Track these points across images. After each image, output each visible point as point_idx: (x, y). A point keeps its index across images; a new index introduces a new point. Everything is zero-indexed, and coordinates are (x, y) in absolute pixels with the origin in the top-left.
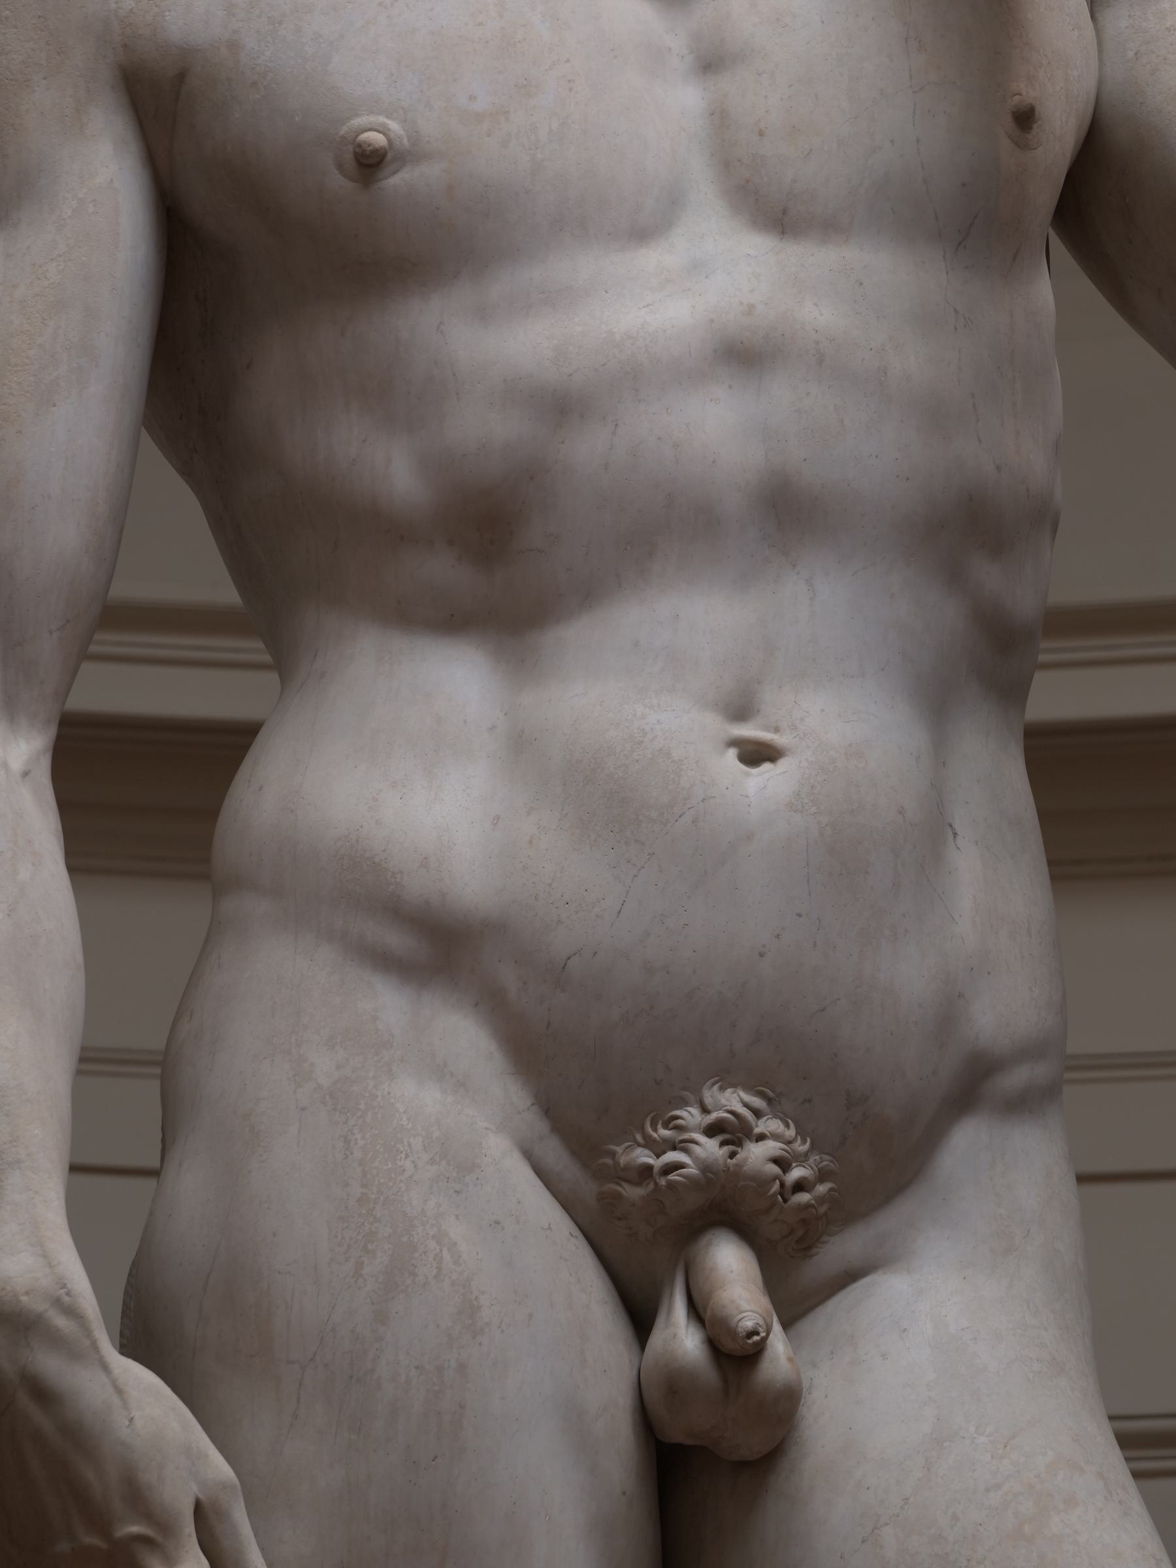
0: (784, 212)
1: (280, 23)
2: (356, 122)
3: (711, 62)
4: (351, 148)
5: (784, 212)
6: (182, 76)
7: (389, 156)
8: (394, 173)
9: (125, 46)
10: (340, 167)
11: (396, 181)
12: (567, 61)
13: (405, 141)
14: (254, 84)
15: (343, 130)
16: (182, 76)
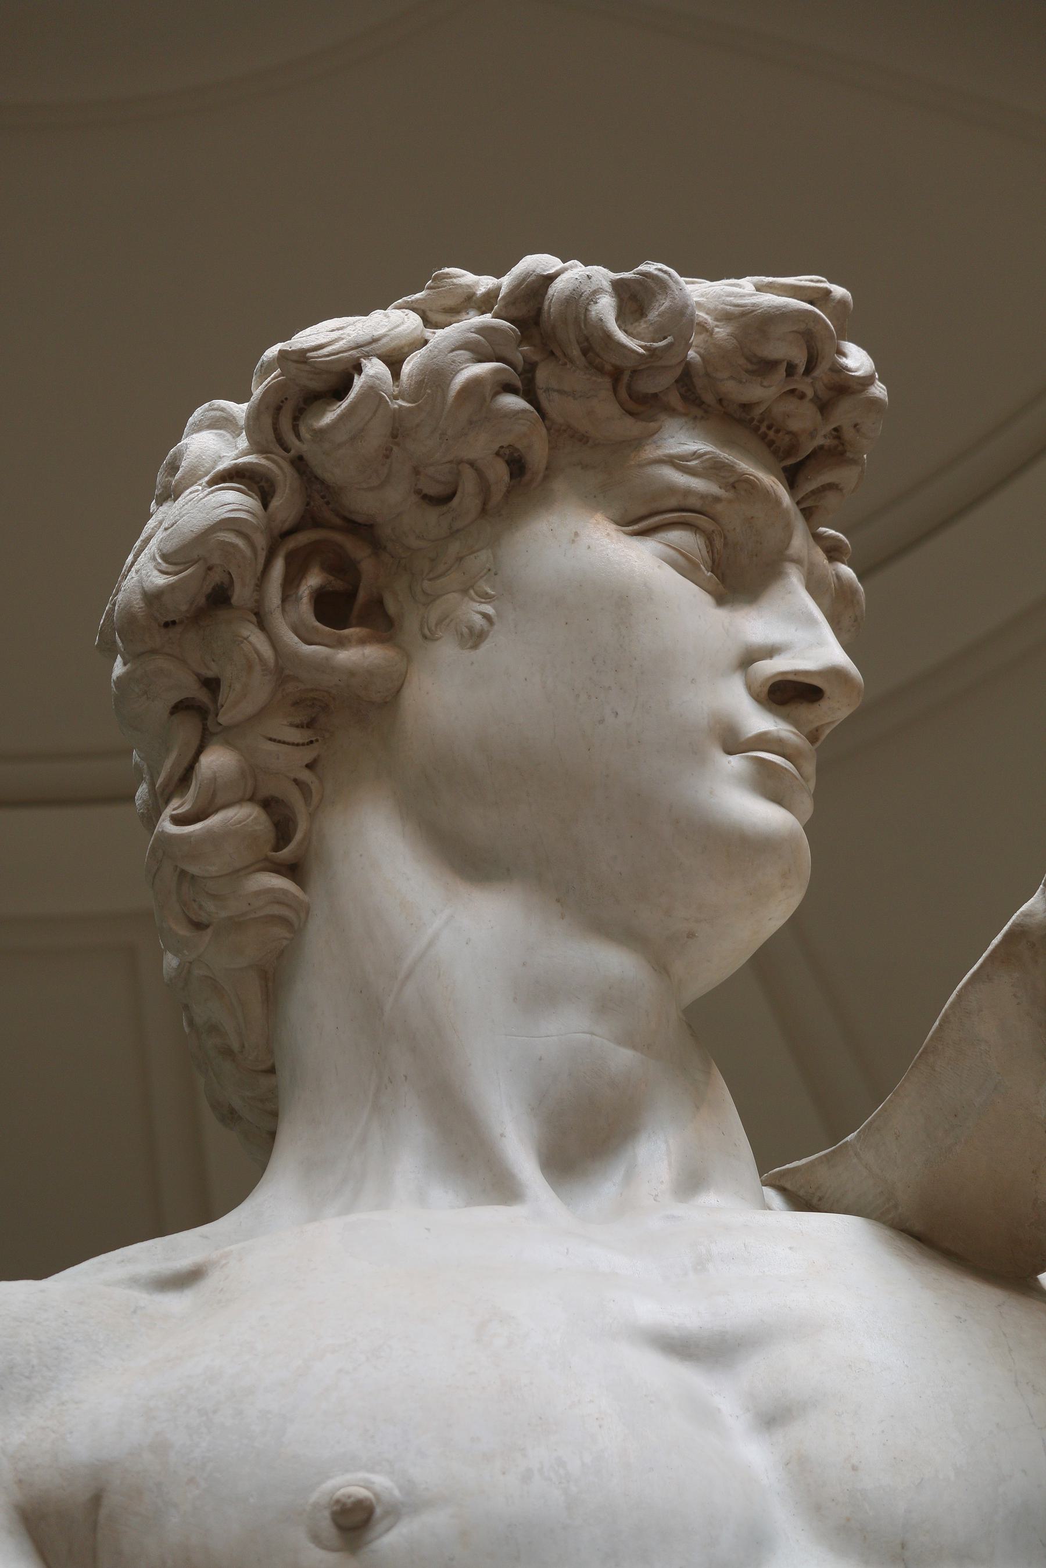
0: (903, 1546)
1: (215, 1412)
2: (328, 1485)
3: (773, 1417)
4: (327, 1513)
5: (903, 1546)
6: (96, 1500)
7: (378, 1511)
8: (388, 1530)
9: (20, 1481)
10: (316, 1539)
11: (390, 1540)
12: (591, 1401)
13: (396, 1493)
14: (191, 1481)
15: (314, 1497)
16: (96, 1500)
